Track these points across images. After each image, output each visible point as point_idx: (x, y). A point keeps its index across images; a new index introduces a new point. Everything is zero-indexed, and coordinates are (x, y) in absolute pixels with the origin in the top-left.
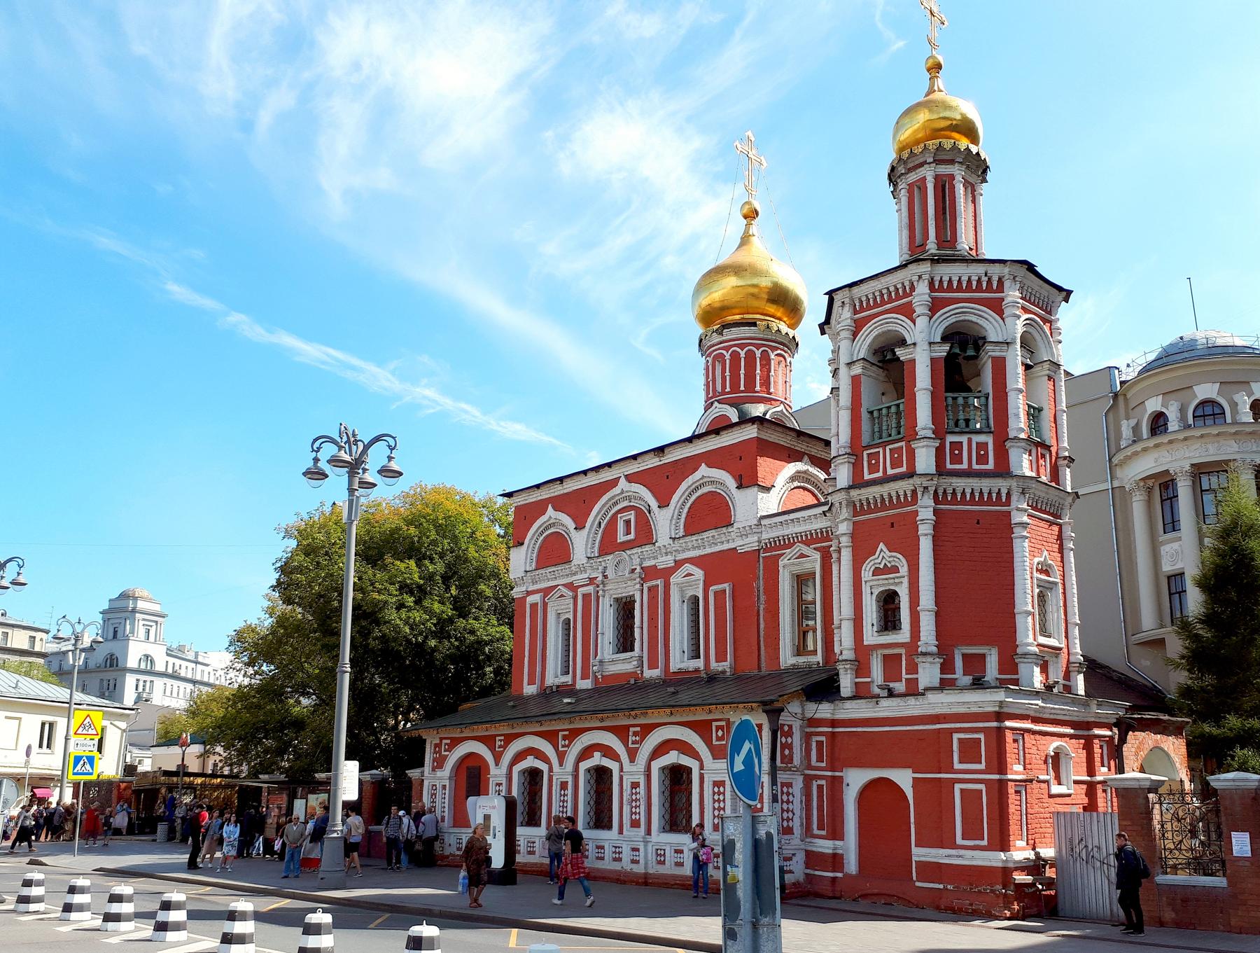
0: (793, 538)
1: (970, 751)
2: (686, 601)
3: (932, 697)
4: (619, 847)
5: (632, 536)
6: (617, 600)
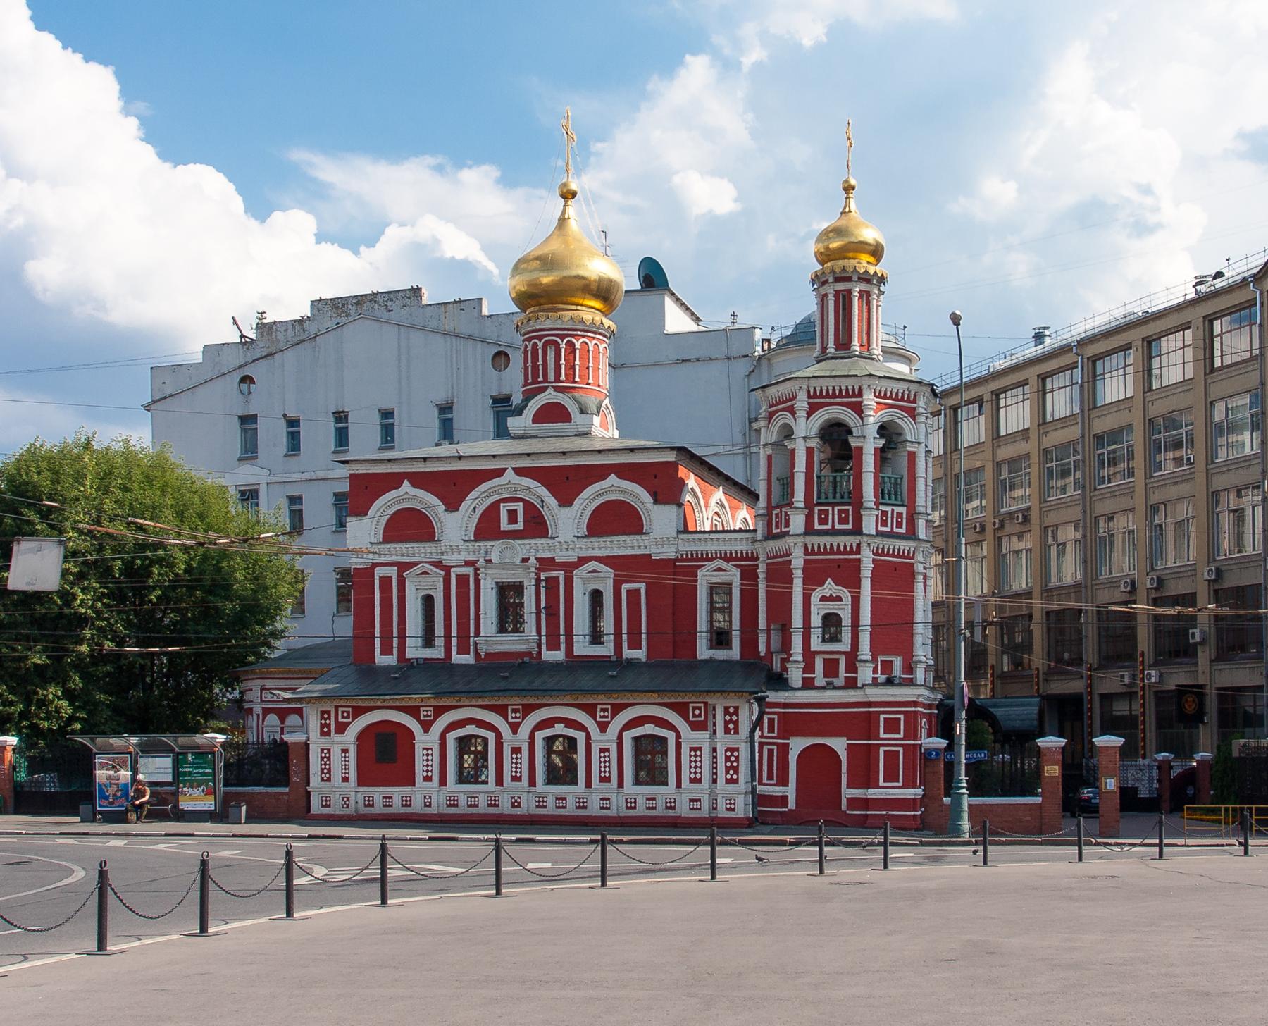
0: (712, 554)
1: (892, 726)
3: (868, 691)
5: (520, 526)
6: (497, 583)
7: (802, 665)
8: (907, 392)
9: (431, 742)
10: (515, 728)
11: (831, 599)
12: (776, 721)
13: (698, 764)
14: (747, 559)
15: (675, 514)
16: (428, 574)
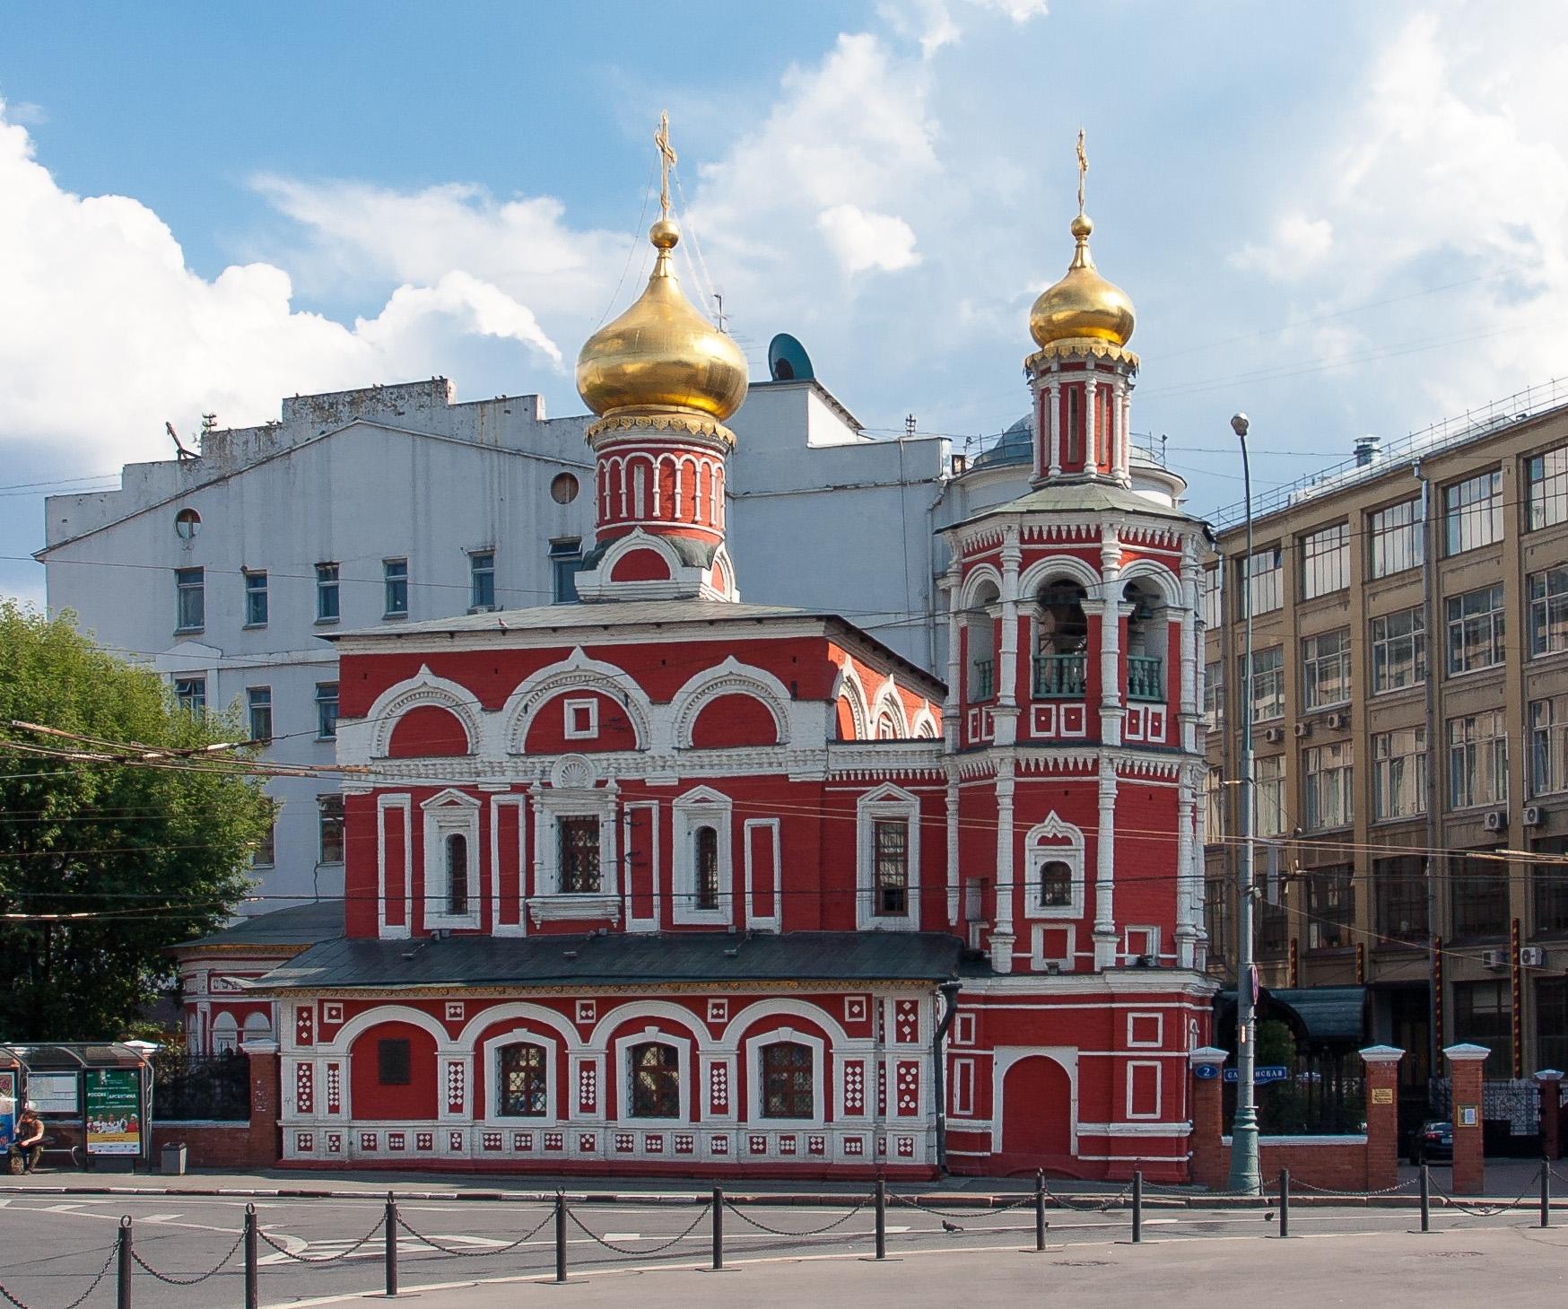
0: (878, 774)
1: (1145, 1030)
4: (687, 1137)
5: (593, 733)
6: (559, 818)
7: (1012, 940)
9: (461, 1053)
10: (585, 1032)
11: (1055, 841)
14: (930, 782)
15: (824, 715)
16: (456, 804)
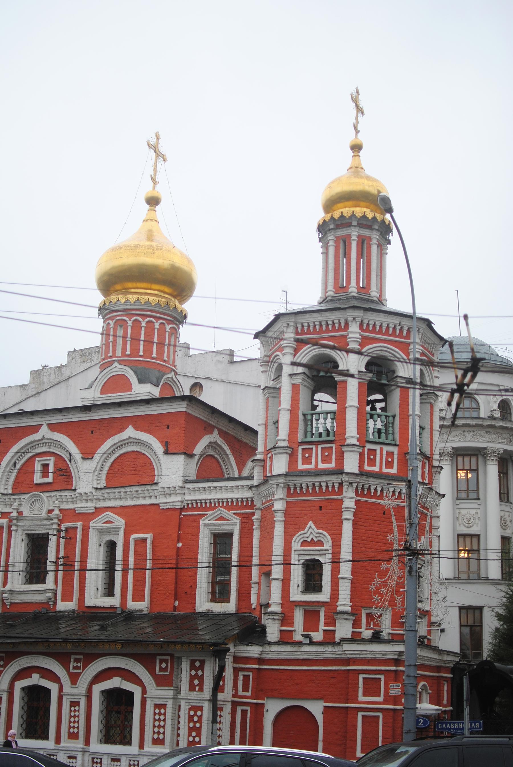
0: (215, 502)
2: (102, 544)
3: (347, 647)
5: (50, 479)
6: (28, 535)
8: (398, 328)
11: (312, 543)
12: (251, 677)
13: (157, 723)
14: (247, 507)
15: (183, 463)
